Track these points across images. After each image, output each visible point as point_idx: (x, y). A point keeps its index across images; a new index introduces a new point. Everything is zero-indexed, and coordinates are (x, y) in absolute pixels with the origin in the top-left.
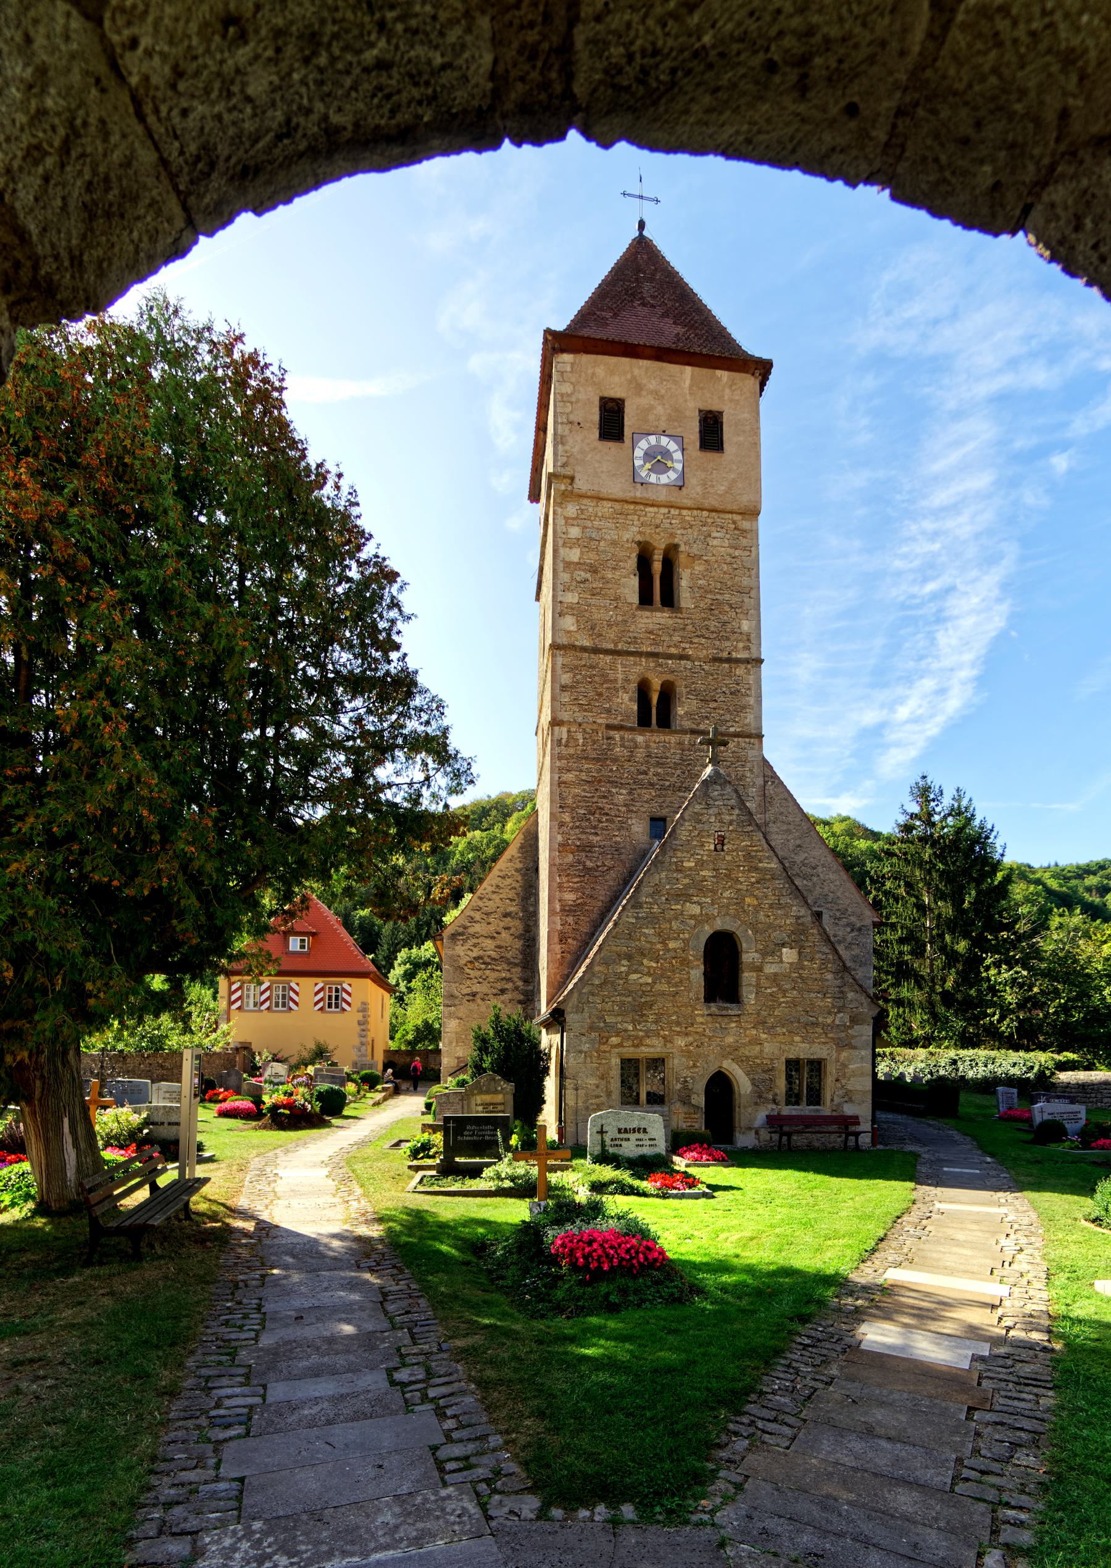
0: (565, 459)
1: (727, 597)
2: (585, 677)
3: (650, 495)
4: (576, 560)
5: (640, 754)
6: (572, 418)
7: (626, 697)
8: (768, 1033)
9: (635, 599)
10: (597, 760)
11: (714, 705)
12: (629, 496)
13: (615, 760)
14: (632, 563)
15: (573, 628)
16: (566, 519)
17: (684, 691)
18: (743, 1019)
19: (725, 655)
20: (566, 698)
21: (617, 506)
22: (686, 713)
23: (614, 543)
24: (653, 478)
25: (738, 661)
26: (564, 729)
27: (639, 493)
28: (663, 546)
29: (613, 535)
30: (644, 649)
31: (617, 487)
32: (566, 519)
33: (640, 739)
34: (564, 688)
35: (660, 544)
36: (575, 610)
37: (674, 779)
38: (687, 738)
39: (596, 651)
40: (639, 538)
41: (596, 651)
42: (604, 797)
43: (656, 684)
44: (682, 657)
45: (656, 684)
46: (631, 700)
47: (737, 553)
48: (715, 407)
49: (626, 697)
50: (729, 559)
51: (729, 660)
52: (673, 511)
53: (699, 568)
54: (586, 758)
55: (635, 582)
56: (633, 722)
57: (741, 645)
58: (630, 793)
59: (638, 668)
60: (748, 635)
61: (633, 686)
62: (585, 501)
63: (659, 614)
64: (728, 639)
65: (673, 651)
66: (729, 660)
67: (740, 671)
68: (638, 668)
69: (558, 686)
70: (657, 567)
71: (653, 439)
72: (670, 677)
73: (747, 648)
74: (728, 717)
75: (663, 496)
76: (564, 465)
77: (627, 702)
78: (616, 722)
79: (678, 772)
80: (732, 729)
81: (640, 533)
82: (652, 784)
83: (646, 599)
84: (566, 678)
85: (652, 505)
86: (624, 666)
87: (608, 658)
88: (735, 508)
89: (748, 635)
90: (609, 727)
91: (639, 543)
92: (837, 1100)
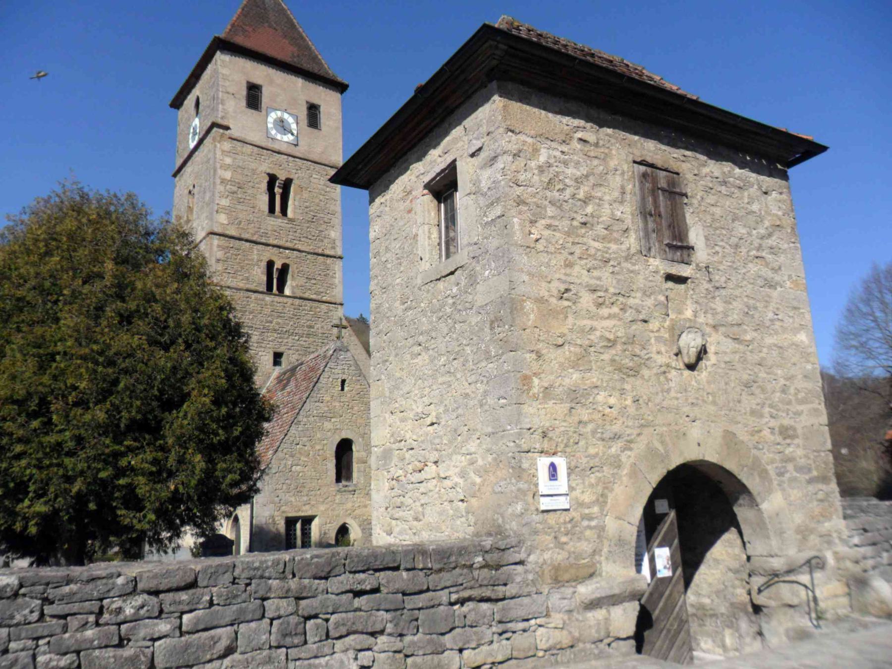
0: (223, 114)
1: (322, 215)
3: (276, 147)
4: (229, 178)
5: (267, 311)
6: (230, 90)
9: (266, 208)
12: (263, 144)
13: (251, 313)
14: (264, 186)
15: (226, 222)
16: (223, 151)
19: (320, 251)
21: (256, 148)
22: (297, 286)
23: (254, 171)
24: (279, 137)
25: (328, 256)
27: (270, 145)
28: (284, 179)
29: (253, 166)
30: (271, 241)
31: (255, 137)
32: (223, 151)
33: (268, 298)
35: (282, 176)
36: (228, 211)
37: (289, 327)
38: (297, 302)
39: (240, 239)
40: (269, 171)
41: (240, 239)
44: (294, 250)
45: (278, 265)
47: (328, 189)
48: (316, 101)
49: (259, 270)
50: (323, 192)
51: (323, 255)
52: (290, 158)
53: (306, 195)
55: (266, 198)
56: (263, 288)
57: (330, 246)
59: (269, 254)
60: (334, 240)
61: (264, 264)
62: (235, 142)
63: (280, 220)
64: (322, 241)
65: (289, 245)
66: (323, 255)
67: (329, 261)
68: (269, 254)
70: (278, 190)
71: (279, 113)
72: (287, 261)
73: (333, 248)
74: (321, 290)
75: (283, 148)
76: (222, 118)
77: (259, 276)
78: (252, 287)
79: (291, 323)
80: (324, 299)
81: (270, 168)
83: (272, 210)
85: (279, 153)
86: (258, 250)
87: (248, 244)
88: (327, 163)
89: (334, 240)
90: (248, 290)
91: (269, 174)
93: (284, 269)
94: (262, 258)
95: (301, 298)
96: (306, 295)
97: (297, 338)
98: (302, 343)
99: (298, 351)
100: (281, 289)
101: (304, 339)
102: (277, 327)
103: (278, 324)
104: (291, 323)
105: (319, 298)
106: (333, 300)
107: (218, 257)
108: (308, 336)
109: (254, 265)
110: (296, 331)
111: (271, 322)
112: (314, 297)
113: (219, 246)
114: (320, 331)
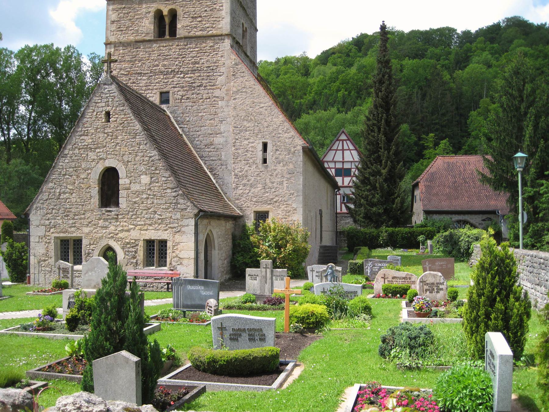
2: (124, 14)
5: (154, 56)
7: (147, 22)
8: (133, 225)
10: (131, 61)
11: (199, 19)
17: (182, 13)
18: (120, 217)
20: (114, 27)
22: (183, 26)
26: (113, 46)
34: (113, 22)
37: (175, 67)
42: (134, 83)
43: (165, 13)
46: (150, 23)
49: (147, 22)
54: (124, 61)
56: (150, 37)
58: (148, 79)
61: (152, 14)
69: (109, 22)
77: (147, 26)
82: (161, 72)
84: (114, 17)
92: (174, 264)
93: (173, 14)
94: (150, 10)
95: (186, 38)
96: (191, 34)
97: (182, 76)
98: (187, 79)
99: (183, 87)
100: (173, 33)
101: (189, 76)
102: (163, 69)
103: (164, 65)
104: (176, 63)
105: (205, 33)
106: (219, 32)
107: (112, 20)
108: (193, 71)
109: (142, 18)
110: (182, 69)
111: (158, 66)
112: (199, 33)
113: (113, 10)
114: (205, 65)
